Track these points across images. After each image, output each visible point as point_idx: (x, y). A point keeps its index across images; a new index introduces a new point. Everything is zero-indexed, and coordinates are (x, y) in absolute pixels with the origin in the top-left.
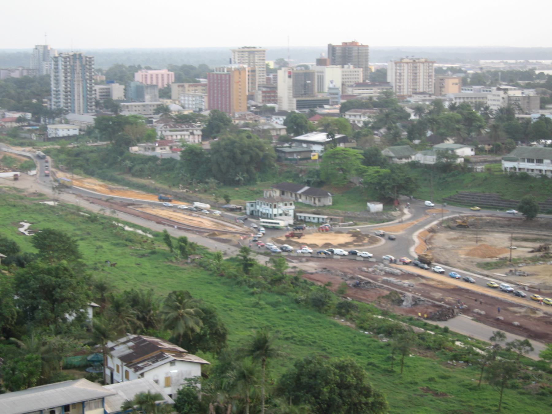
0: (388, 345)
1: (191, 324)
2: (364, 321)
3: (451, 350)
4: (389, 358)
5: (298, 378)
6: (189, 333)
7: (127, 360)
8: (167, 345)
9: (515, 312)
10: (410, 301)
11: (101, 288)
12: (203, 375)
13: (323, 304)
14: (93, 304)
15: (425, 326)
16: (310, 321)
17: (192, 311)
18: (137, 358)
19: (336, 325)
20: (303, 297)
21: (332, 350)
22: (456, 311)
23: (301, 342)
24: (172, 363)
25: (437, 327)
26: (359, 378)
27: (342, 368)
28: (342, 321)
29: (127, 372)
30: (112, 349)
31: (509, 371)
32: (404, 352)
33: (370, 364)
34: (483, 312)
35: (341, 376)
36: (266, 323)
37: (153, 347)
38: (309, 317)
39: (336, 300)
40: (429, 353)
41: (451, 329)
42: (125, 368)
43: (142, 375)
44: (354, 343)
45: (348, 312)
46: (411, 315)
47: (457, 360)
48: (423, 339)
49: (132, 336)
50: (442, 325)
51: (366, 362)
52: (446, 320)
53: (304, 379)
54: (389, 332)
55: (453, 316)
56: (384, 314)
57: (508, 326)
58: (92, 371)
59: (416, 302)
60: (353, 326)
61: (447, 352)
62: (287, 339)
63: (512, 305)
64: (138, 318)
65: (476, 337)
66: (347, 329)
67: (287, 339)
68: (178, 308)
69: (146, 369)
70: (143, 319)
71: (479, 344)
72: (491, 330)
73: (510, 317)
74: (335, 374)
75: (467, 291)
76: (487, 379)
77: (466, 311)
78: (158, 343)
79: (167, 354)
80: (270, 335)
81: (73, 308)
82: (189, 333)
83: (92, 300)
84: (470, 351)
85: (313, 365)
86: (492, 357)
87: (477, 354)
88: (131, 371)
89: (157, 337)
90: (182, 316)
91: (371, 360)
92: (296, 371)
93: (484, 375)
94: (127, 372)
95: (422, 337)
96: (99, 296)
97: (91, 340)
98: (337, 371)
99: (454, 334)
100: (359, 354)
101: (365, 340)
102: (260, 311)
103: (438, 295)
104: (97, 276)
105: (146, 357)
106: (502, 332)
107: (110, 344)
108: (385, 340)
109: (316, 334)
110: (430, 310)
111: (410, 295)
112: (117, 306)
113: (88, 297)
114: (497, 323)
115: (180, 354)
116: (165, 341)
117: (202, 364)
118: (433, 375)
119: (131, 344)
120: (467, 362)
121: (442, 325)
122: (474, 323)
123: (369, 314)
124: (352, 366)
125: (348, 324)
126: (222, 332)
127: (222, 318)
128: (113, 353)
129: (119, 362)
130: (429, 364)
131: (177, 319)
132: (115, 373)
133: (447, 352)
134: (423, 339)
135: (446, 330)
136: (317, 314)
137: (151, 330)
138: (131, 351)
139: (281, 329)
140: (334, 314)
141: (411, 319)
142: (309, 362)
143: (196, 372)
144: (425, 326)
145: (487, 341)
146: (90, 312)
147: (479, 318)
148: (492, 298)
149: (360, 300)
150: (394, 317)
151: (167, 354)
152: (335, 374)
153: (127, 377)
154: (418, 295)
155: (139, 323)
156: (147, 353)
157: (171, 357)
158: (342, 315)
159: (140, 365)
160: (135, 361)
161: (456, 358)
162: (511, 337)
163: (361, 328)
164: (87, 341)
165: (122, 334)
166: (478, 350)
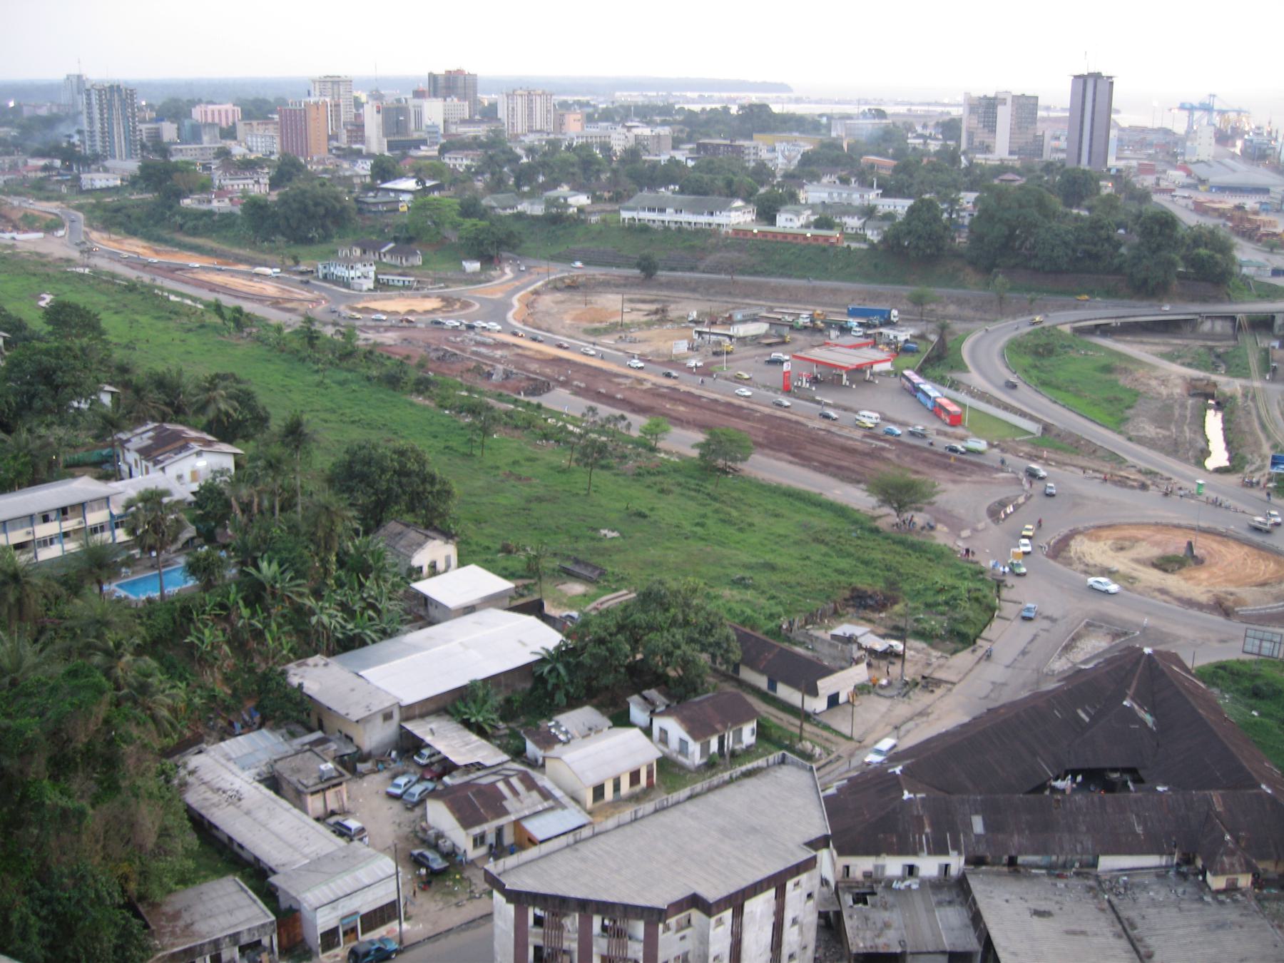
0: (470, 425)
1: (223, 406)
2: (444, 399)
3: (541, 429)
4: (470, 440)
5: (350, 465)
6: (225, 419)
7: (146, 453)
8: (193, 434)
9: (619, 384)
10: (501, 373)
11: (123, 369)
12: (237, 466)
13: (398, 380)
14: (108, 388)
15: (516, 402)
16: (383, 401)
17: (223, 393)
18: (156, 449)
19: (412, 404)
20: (375, 373)
21: (406, 433)
22: (552, 384)
23: (370, 425)
24: (199, 454)
25: (529, 404)
26: (422, 463)
27: (402, 453)
28: (420, 400)
29: (147, 468)
30: (128, 441)
31: (602, 450)
32: (486, 431)
33: (447, 447)
34: (583, 385)
35: (400, 462)
36: (329, 405)
37: (177, 436)
38: (382, 396)
39: (414, 374)
40: (517, 433)
41: (544, 404)
42: (144, 463)
43: (163, 469)
44: (431, 424)
45: (427, 389)
46: (500, 390)
47: (547, 440)
48: (511, 417)
49: (151, 425)
50: (534, 400)
51: (442, 445)
52: (540, 395)
53: (358, 468)
54: (473, 410)
55: (549, 389)
56: (470, 390)
57: (609, 399)
58: (108, 468)
59: (507, 375)
60: (432, 405)
61: (538, 431)
62: (353, 422)
63: (617, 375)
64: (167, 404)
65: (572, 413)
66: (425, 408)
67: (353, 422)
68: (208, 390)
69: (167, 462)
70: (170, 404)
71: (574, 421)
72: (582, 403)
73: (613, 389)
74: (392, 460)
75: (568, 361)
76: (577, 461)
77: (564, 384)
78: (183, 432)
79: (193, 444)
80: (305, 417)
81: (81, 395)
82: (225, 419)
83: (110, 384)
84: (563, 429)
85: (365, 451)
86: (581, 436)
87: (572, 433)
88: (150, 465)
89: (182, 423)
90: (214, 399)
91: (450, 444)
92: (347, 457)
93: (575, 456)
94: (147, 468)
95: (509, 414)
96: (118, 379)
97: (95, 432)
98: (395, 456)
99: (548, 411)
100: (435, 437)
101: (444, 421)
102: (323, 391)
103: (534, 366)
104: (118, 355)
105: (168, 448)
106: (594, 404)
107: (123, 436)
108: (469, 420)
109: (387, 416)
110: (523, 384)
111: (500, 367)
112: (138, 391)
113: (99, 382)
114: (600, 397)
115: (209, 443)
116: (194, 427)
117: (235, 454)
118: (518, 457)
119: (151, 434)
120: (558, 441)
121: (534, 400)
122: (573, 398)
123: (451, 391)
124: (413, 450)
125: (427, 402)
126: (263, 414)
127: (262, 399)
128: (128, 445)
129: (137, 456)
130: (515, 445)
131: (208, 402)
132: (134, 469)
133: (538, 431)
134: (511, 417)
135: (539, 406)
136: (391, 392)
137: (181, 418)
138: (150, 442)
139: (347, 411)
140: (411, 392)
141: (500, 395)
142: (361, 448)
143: (229, 463)
144: (516, 402)
145: (578, 415)
146: (106, 399)
147: (578, 392)
148: (596, 369)
149: (443, 375)
150: (481, 393)
151: (193, 444)
152: (392, 460)
153: (147, 472)
154: (512, 368)
155: (168, 410)
156: (168, 444)
157: (196, 447)
158: (419, 392)
159: (160, 458)
160: (154, 454)
161: (546, 437)
162: (605, 410)
163: (441, 406)
164: (91, 433)
165: (140, 421)
166: (571, 428)
